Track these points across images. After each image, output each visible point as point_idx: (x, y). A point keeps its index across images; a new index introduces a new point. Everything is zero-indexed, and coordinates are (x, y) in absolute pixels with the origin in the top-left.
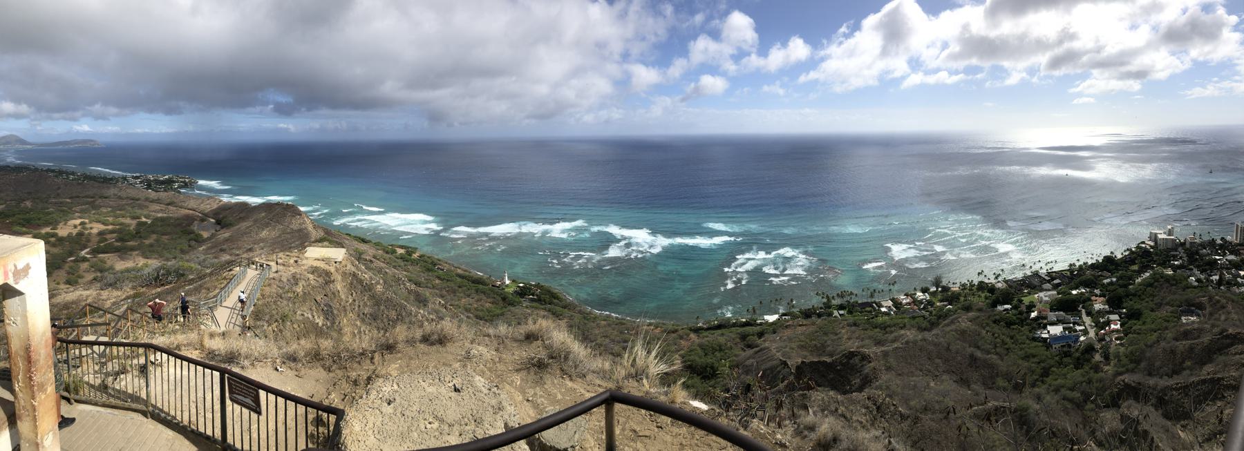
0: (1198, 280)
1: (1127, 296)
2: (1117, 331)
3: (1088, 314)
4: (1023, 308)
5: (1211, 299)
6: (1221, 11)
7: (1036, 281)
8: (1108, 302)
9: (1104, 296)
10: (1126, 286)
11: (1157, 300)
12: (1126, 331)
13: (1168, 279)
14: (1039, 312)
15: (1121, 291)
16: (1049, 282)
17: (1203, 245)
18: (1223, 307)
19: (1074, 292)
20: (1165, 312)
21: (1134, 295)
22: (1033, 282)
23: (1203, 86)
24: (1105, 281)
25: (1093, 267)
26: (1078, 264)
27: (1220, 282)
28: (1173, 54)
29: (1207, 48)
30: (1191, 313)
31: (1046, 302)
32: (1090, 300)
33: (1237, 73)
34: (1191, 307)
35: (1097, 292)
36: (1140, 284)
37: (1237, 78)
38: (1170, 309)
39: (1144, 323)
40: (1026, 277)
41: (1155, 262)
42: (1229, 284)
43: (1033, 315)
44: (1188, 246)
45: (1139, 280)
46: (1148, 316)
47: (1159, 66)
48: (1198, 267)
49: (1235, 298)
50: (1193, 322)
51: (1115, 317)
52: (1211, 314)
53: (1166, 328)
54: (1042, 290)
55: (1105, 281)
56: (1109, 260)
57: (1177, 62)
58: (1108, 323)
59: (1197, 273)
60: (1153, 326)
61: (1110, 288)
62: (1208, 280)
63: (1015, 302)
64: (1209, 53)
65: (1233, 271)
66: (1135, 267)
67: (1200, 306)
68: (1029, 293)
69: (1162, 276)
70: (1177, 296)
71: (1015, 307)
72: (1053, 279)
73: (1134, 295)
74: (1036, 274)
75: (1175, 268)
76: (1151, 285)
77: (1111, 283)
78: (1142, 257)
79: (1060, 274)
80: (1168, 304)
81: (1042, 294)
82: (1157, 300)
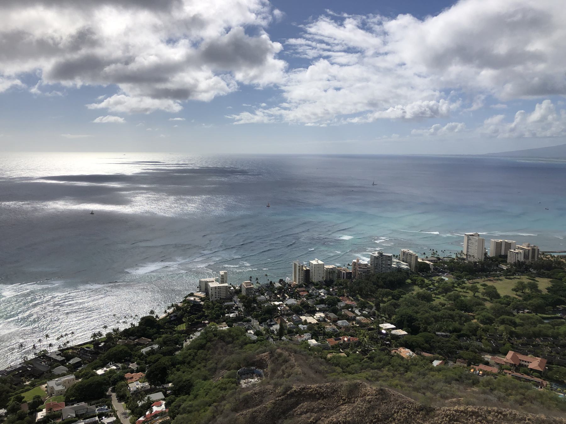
0: (257, 333)
1: (173, 365)
2: (161, 414)
3: (121, 398)
4: (25, 409)
5: (272, 353)
6: (265, 36)
7: (43, 366)
8: (149, 378)
9: (142, 370)
10: (171, 353)
11: (211, 364)
12: (173, 411)
13: (222, 337)
14: (49, 410)
15: (165, 360)
16: (63, 363)
17: (260, 291)
18: (286, 361)
19: (100, 372)
20: (221, 377)
21: (183, 363)
22: (39, 368)
23: (253, 112)
24: (144, 350)
25: (127, 333)
26: (104, 333)
27: (281, 333)
28: (217, 74)
29: (253, 72)
30: (250, 374)
31: (60, 393)
32: (122, 378)
33: (284, 100)
34: (251, 367)
35: (133, 366)
36: (189, 348)
37: (285, 105)
38: (226, 373)
39: (196, 397)
40: (27, 362)
41: (206, 317)
42: (290, 332)
43: (40, 415)
44: (244, 293)
45: (188, 342)
46: (201, 386)
47: (203, 85)
48: (256, 317)
49: (298, 348)
50: (254, 385)
51: (160, 395)
52: (273, 372)
53: (223, 398)
54: (52, 377)
55: (144, 350)
56: (148, 322)
57: (223, 84)
58: (149, 406)
59: (255, 323)
60: (207, 399)
61: (153, 358)
62: (267, 331)
63: (11, 402)
64: (255, 77)
65: (294, 317)
66: (182, 327)
67: (261, 364)
68: (33, 385)
69: (216, 333)
70: (233, 356)
71: (12, 411)
72: (69, 358)
73: (183, 363)
74: (44, 356)
75: (230, 322)
76: (202, 347)
77: (152, 352)
78: (190, 313)
79: (80, 350)
80: (223, 367)
81: (52, 383)
82: (211, 364)
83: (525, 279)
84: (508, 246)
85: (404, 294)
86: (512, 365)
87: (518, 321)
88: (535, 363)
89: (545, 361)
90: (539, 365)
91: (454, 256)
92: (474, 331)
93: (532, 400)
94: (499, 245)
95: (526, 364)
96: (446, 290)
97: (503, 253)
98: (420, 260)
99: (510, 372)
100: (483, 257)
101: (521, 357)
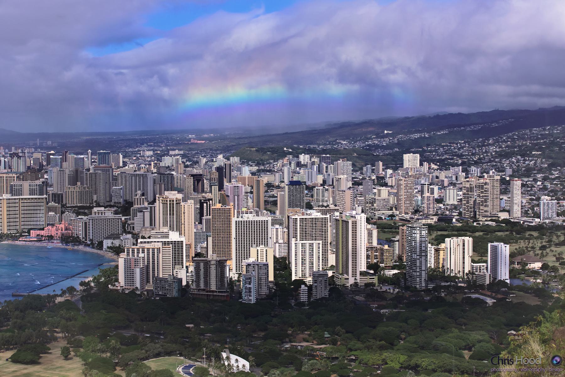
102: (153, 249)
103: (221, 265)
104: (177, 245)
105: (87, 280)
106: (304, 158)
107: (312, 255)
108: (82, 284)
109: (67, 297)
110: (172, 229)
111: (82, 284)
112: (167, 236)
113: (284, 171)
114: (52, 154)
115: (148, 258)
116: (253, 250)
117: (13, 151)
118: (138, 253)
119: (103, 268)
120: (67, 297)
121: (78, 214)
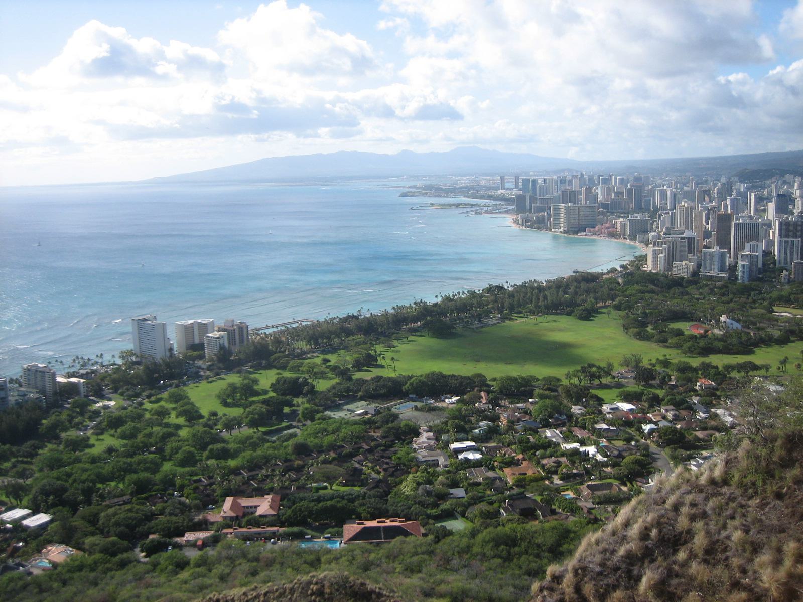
83: (233, 378)
84: (204, 328)
85: (42, 448)
86: (232, 518)
87: (232, 446)
88: (264, 506)
89: (278, 497)
90: (271, 507)
91: (120, 362)
92: (169, 482)
93: (270, 564)
94: (188, 330)
95: (253, 510)
96: (115, 423)
97: (197, 341)
98: (60, 379)
99: (231, 530)
100: (168, 354)
101: (245, 502)
102: (673, 243)
103: (723, 256)
104: (690, 240)
105: (625, 263)
106: (788, 177)
107: (792, 248)
108: (622, 267)
109: (611, 275)
110: (687, 228)
111: (622, 267)
112: (683, 233)
113: (773, 188)
114: (602, 176)
115: (669, 248)
116: (747, 246)
117: (575, 174)
118: (662, 244)
119: (637, 254)
120: (611, 275)
121: (620, 217)
